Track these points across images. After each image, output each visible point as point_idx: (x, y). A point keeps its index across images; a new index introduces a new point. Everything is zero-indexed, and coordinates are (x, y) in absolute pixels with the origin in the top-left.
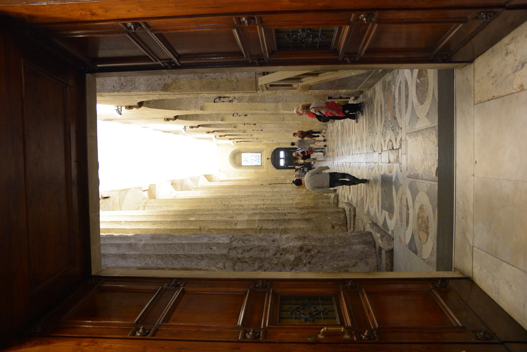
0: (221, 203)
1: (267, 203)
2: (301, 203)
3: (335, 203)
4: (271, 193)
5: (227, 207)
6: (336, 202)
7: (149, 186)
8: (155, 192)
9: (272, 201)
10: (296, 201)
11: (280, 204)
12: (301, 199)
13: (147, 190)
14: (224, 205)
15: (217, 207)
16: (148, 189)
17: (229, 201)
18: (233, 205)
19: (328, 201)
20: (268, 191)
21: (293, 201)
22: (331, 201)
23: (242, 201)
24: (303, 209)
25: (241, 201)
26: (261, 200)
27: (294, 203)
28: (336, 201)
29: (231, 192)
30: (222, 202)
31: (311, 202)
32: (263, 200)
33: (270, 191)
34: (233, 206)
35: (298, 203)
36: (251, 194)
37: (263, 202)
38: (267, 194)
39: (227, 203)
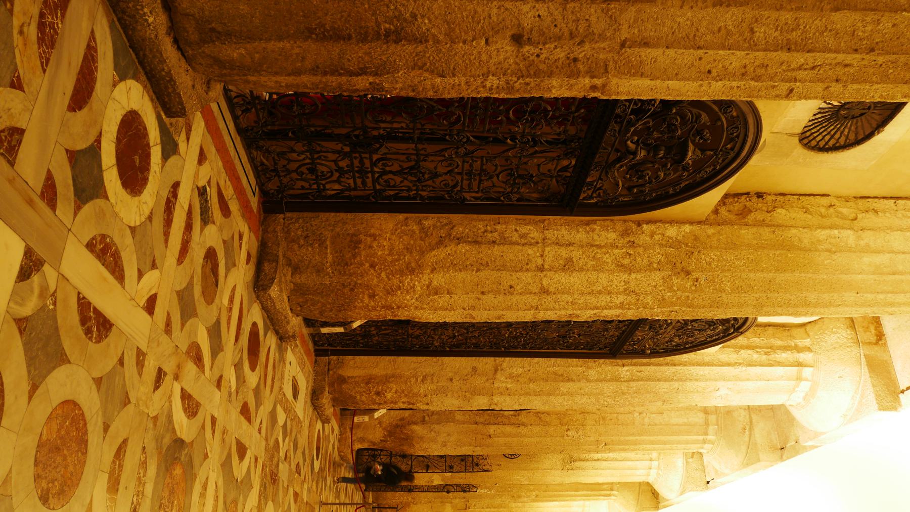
0: (697, 280)
1: (530, 274)
2: (402, 273)
3: (269, 261)
4: (498, 388)
5: (678, 264)
6: (266, 264)
7: (900, 405)
8: (874, 386)
9: (511, 287)
10: (420, 283)
11: (482, 268)
12: (399, 288)
13: (903, 392)
14: (688, 273)
15: (713, 265)
16: (901, 395)
17: (670, 289)
18: (655, 269)
19: (297, 279)
20: (508, 397)
21: (430, 283)
22: (289, 277)
23: (622, 289)
24: (388, 33)
25: (625, 290)
26: (552, 289)
27: (429, 271)
28: (266, 266)
29: (623, 393)
30: (693, 288)
31: (362, 276)
32: (545, 291)
33: (502, 394)
34: (655, 265)
35: (412, 272)
36: (561, 384)
37: (545, 282)
38: (509, 386)
39: (675, 280)
